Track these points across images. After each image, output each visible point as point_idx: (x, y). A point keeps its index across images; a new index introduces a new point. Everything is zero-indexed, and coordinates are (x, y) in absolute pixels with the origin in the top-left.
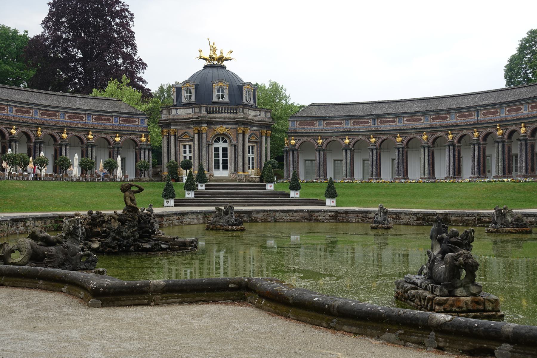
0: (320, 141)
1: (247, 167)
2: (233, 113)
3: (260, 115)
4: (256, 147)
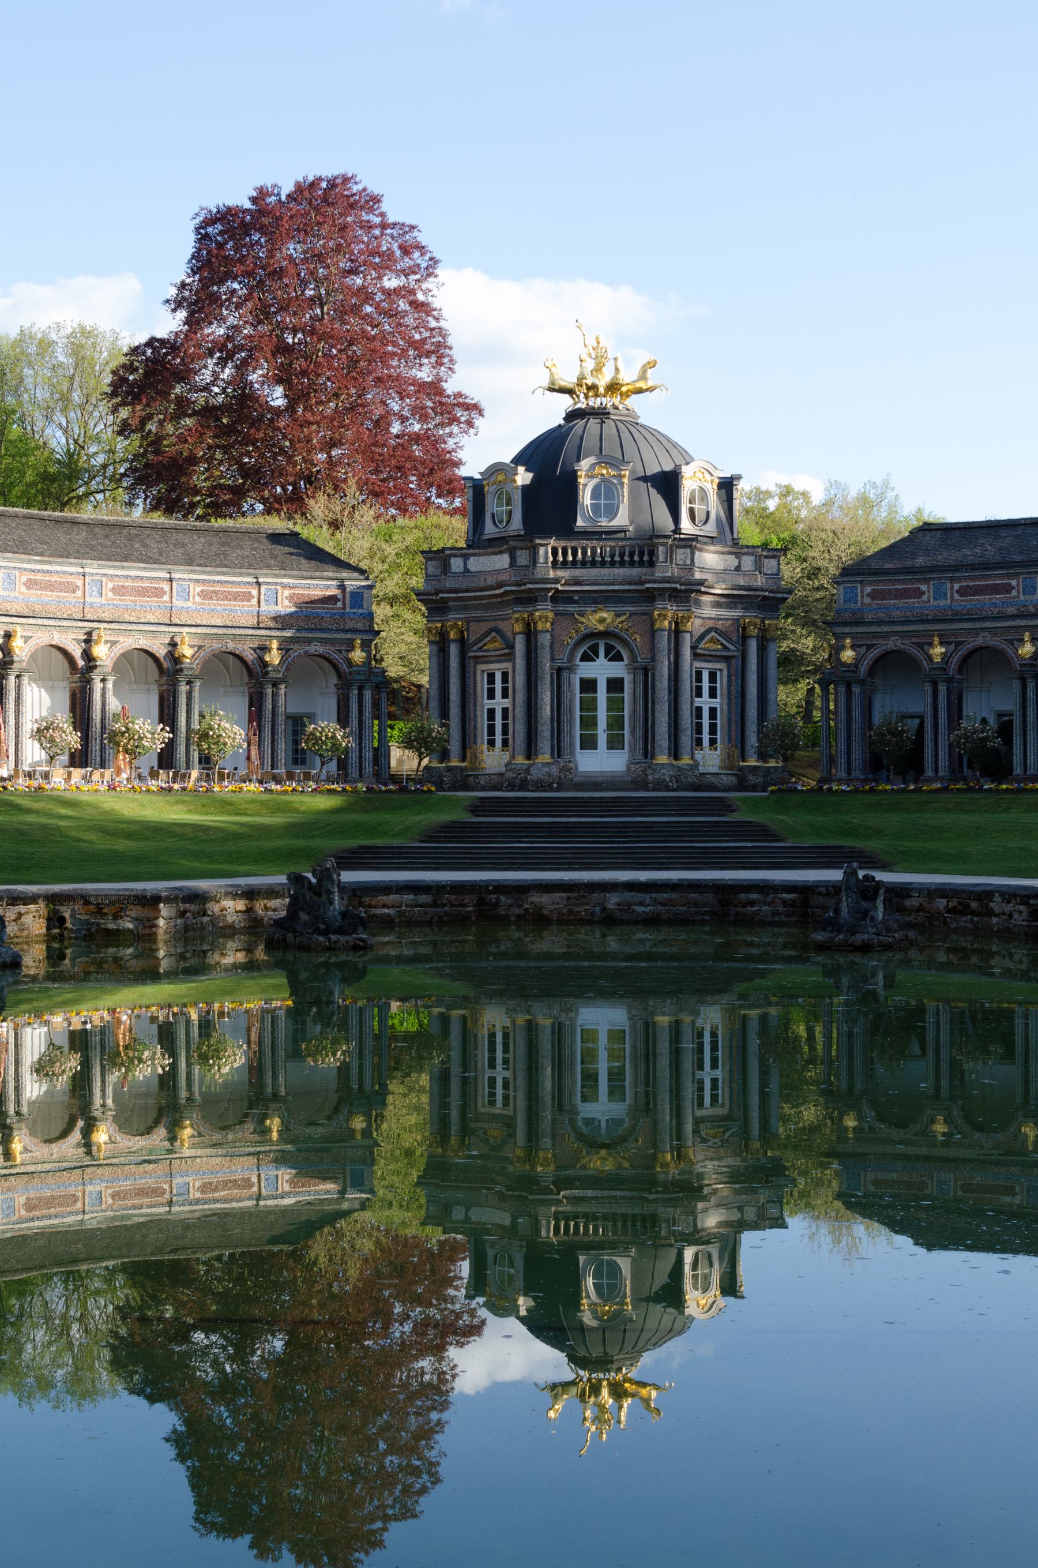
0: (938, 651)
1: (686, 740)
2: (641, 564)
3: (738, 569)
4: (725, 673)
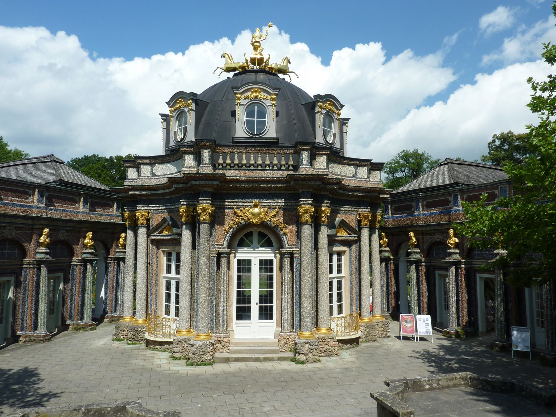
3: (355, 176)
4: (347, 253)
